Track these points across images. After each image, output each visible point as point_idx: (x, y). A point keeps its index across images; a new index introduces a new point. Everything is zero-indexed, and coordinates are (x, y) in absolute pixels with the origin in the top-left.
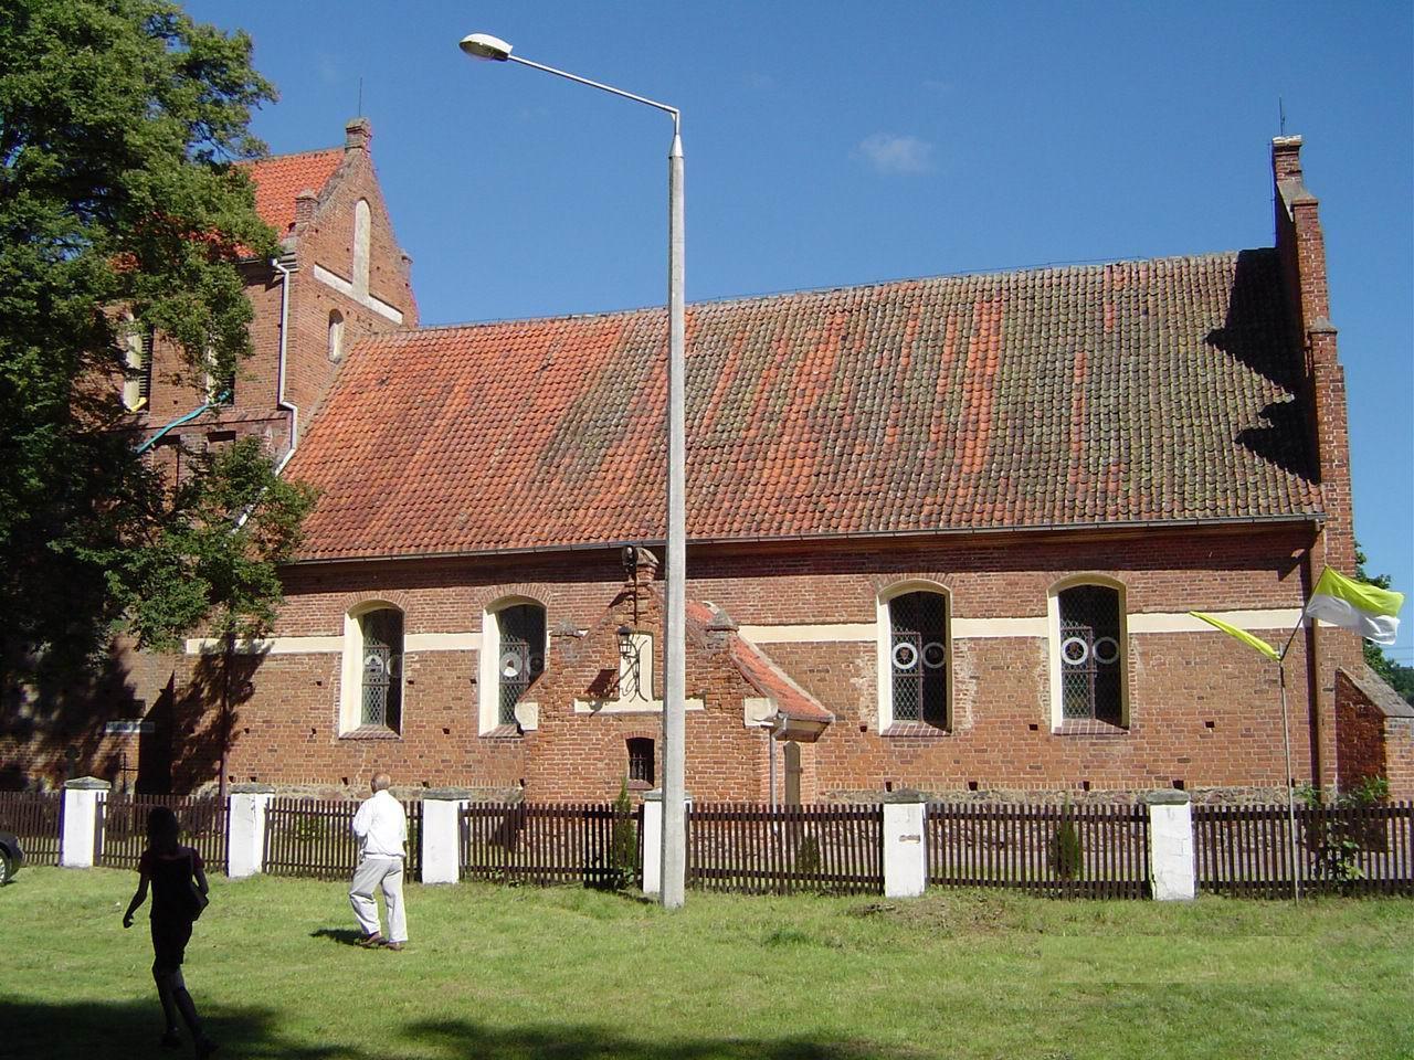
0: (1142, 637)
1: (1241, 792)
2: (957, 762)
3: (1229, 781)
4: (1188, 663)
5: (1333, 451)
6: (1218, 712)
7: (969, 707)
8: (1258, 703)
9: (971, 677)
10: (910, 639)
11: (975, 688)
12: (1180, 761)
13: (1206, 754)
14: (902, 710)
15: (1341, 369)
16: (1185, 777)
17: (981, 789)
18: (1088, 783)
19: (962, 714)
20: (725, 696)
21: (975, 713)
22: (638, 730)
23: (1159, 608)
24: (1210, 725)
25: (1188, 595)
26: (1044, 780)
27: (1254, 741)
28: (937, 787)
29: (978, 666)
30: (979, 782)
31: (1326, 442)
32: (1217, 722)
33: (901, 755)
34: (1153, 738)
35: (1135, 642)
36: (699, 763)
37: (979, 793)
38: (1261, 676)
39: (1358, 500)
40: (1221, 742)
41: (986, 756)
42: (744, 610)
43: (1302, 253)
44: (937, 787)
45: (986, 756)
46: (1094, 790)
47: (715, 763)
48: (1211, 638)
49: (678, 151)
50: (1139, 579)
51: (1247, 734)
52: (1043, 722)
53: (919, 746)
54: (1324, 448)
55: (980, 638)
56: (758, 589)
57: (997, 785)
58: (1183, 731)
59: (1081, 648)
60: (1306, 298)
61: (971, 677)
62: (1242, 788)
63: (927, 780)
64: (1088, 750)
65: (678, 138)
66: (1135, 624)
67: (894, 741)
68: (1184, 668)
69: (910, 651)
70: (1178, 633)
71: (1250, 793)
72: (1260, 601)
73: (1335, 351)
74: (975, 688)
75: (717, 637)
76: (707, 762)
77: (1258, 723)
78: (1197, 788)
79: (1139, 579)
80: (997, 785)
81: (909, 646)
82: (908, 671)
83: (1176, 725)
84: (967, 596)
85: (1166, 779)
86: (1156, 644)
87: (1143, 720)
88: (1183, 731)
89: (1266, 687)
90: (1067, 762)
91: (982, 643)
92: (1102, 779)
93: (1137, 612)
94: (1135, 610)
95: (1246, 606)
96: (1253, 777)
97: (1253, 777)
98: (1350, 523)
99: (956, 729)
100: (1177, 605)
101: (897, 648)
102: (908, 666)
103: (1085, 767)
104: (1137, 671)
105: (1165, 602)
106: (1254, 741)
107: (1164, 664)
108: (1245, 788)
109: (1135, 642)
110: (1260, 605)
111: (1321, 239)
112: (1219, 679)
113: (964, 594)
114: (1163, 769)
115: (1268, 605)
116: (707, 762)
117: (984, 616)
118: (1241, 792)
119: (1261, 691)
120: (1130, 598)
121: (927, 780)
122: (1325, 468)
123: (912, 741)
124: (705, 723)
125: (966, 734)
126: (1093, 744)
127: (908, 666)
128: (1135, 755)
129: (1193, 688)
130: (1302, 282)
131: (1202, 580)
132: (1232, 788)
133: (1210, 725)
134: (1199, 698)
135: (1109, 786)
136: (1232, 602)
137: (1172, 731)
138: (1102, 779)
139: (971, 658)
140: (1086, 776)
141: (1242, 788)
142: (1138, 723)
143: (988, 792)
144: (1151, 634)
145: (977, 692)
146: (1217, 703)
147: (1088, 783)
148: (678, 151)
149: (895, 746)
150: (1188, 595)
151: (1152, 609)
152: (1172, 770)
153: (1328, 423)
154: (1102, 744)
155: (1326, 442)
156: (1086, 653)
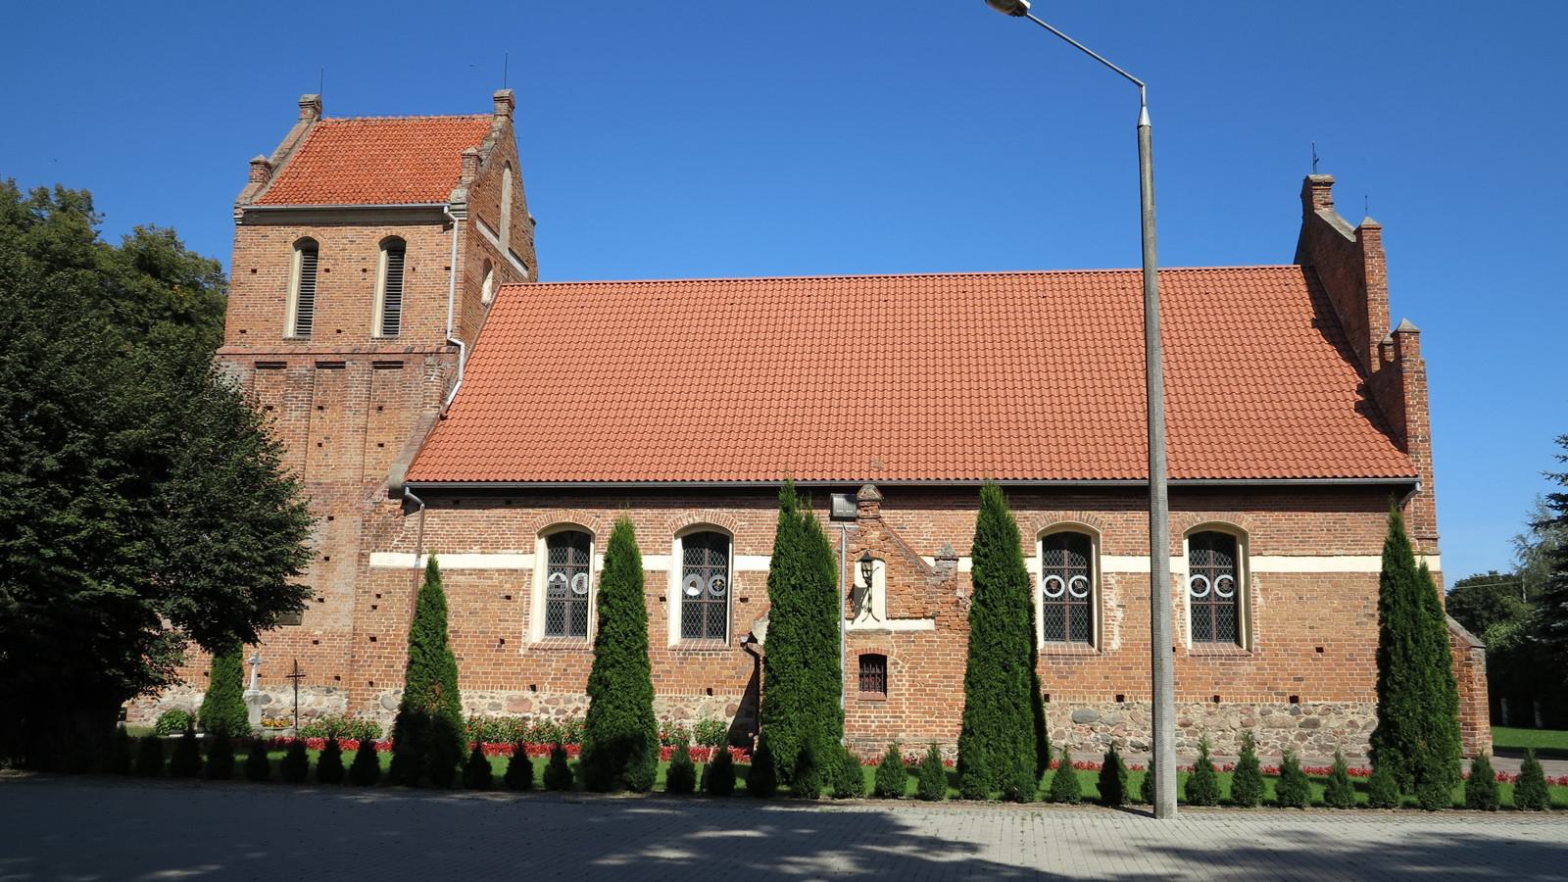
0: (1263, 576)
1: (1347, 707)
2: (1106, 678)
3: (1336, 698)
4: (1300, 598)
5: (1417, 429)
6: (1326, 640)
7: (1116, 631)
8: (1358, 633)
9: (1118, 606)
10: (1204, 571)
11: (1122, 616)
12: (1295, 679)
13: (1316, 674)
14: (1200, 633)
15: (1422, 363)
16: (1300, 692)
17: (1127, 701)
18: (1218, 697)
19: (1111, 636)
20: (955, 618)
21: (1122, 636)
22: (871, 646)
23: (1276, 552)
24: (1320, 650)
25: (1301, 542)
26: (1182, 693)
27: (1357, 664)
28: (1090, 700)
29: (1124, 596)
30: (1126, 695)
31: (1411, 421)
32: (1325, 648)
33: (1058, 671)
34: (1273, 660)
35: (1256, 580)
36: (930, 677)
37: (1126, 705)
38: (1361, 611)
39: (1435, 469)
40: (1330, 664)
41: (1132, 673)
42: (917, 543)
43: (1368, 268)
44: (1090, 700)
45: (1132, 673)
46: (1224, 703)
47: (945, 677)
48: (1320, 578)
49: (1145, 121)
50: (1259, 527)
51: (1351, 659)
52: (1180, 645)
53: (1074, 663)
54: (1410, 426)
55: (1126, 573)
56: (929, 526)
57: (1141, 698)
58: (1297, 655)
59: (1205, 584)
60: (1371, 305)
61: (1118, 606)
62: (1347, 703)
63: (1080, 693)
64: (1218, 669)
65: (1144, 108)
66: (1257, 564)
67: (1052, 659)
68: (1298, 603)
69: (1059, 583)
70: (1292, 573)
71: (1354, 707)
72: (1360, 549)
73: (1417, 347)
74: (1122, 616)
75: (945, 566)
76: (936, 677)
77: (1359, 650)
78: (1310, 702)
79: (1259, 527)
80: (1141, 698)
81: (1057, 577)
82: (1056, 599)
83: (1291, 650)
84: (1114, 537)
85: (1283, 694)
86: (1274, 582)
87: (1263, 645)
88: (1297, 655)
89: (1365, 620)
90: (1200, 679)
91: (1127, 577)
92: (1230, 694)
93: (1258, 555)
94: (1256, 553)
95: (1347, 552)
96: (1356, 694)
97: (1356, 694)
98: (1432, 488)
99: (1106, 650)
100: (1292, 550)
101: (1047, 579)
102: (1057, 595)
103: (1216, 683)
104: (1259, 606)
105: (1280, 548)
106: (1357, 664)
107: (1281, 598)
108: (1350, 703)
109: (1256, 580)
110: (1359, 552)
111: (1383, 257)
112: (1325, 612)
113: (1112, 535)
114: (1281, 686)
115: (1366, 552)
116: (936, 677)
117: (1129, 555)
118: (1347, 707)
119: (1362, 623)
120: (1255, 539)
121: (1080, 693)
122: (1411, 443)
123: (1068, 659)
124: (936, 642)
125: (1115, 653)
126: (1222, 664)
127: (1057, 595)
128: (1258, 674)
129: (1306, 619)
130: (1369, 291)
131: (1310, 530)
132: (1339, 703)
133: (1320, 650)
134: (1310, 628)
135: (1236, 700)
136: (1337, 549)
137: (1288, 655)
138: (1230, 694)
139: (1117, 590)
140: (1217, 691)
141: (1347, 703)
142: (1260, 648)
143: (1133, 704)
144: (1270, 573)
145: (1123, 619)
146: (1323, 632)
147: (1218, 697)
148: (1145, 121)
149: (1053, 663)
150: (1301, 542)
151: (1271, 552)
152: (1288, 687)
153: (1413, 406)
154: (1230, 664)
155: (1411, 421)
156: (1208, 588)
